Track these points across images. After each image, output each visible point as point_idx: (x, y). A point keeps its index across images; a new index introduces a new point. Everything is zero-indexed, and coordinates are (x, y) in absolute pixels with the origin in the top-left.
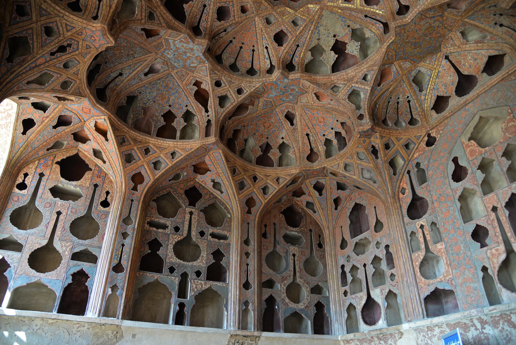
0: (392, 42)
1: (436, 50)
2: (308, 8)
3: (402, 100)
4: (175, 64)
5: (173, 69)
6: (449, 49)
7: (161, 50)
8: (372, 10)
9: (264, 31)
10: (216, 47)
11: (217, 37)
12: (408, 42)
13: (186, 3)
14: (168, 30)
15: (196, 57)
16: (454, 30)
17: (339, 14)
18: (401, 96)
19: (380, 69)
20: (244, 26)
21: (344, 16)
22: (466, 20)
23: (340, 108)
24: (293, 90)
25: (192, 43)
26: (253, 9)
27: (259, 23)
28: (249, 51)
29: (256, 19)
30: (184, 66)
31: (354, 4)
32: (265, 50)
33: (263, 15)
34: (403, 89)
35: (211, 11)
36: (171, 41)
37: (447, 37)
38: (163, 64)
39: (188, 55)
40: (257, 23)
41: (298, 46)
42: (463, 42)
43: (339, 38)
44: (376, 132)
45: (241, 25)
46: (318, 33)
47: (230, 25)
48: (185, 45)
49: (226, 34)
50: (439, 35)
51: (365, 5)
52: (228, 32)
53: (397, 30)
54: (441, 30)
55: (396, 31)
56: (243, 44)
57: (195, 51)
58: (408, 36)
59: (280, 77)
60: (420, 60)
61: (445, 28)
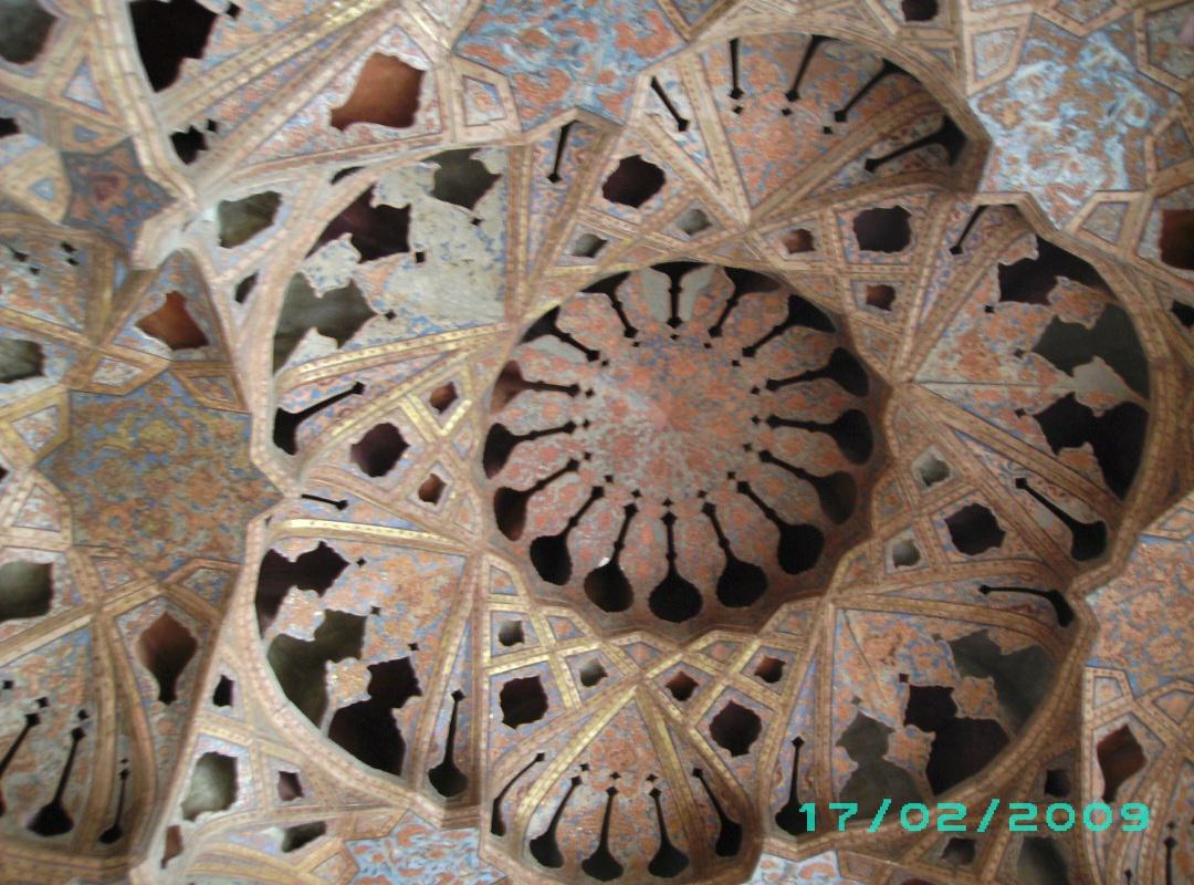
0: (247, 440)
1: (57, 462)
2: (561, 295)
3: (13, 274)
4: (1112, 53)
5: (1126, 20)
6: (22, 495)
7: (1166, 122)
8: (358, 427)
9: (709, 185)
10: (908, 104)
11: (908, 140)
12: (184, 457)
13: (1026, 261)
14: (1130, 259)
15: (1019, 120)
16: (72, 555)
17: (448, 336)
18: (32, 281)
19: (224, 348)
20: (793, 186)
21: (427, 341)
22: (86, 620)
23: (278, 119)
24: (530, 42)
25: (1037, 192)
26: (764, 245)
27: (733, 206)
28: (757, 89)
29: (745, 216)
30: (1073, 49)
31: (419, 396)
32: (685, 113)
33: (725, 234)
34: (50, 308)
35: (934, 240)
36: (1120, 182)
37: (67, 522)
38: (1168, 46)
39: (1052, 127)
40: (742, 201)
41: (554, 178)
42: (10, 555)
43: (399, 259)
44: (68, 220)
45: (806, 189)
46: (490, 242)
47: (851, 189)
48: (1065, 177)
49: (867, 150)
50: (104, 518)
51: (384, 420)
52: (856, 158)
53: (270, 489)
54: (112, 535)
55: (269, 483)
56: (786, 112)
57: (1020, 153)
58: (209, 478)
59: (623, 107)
60: (79, 407)
61: (106, 547)
